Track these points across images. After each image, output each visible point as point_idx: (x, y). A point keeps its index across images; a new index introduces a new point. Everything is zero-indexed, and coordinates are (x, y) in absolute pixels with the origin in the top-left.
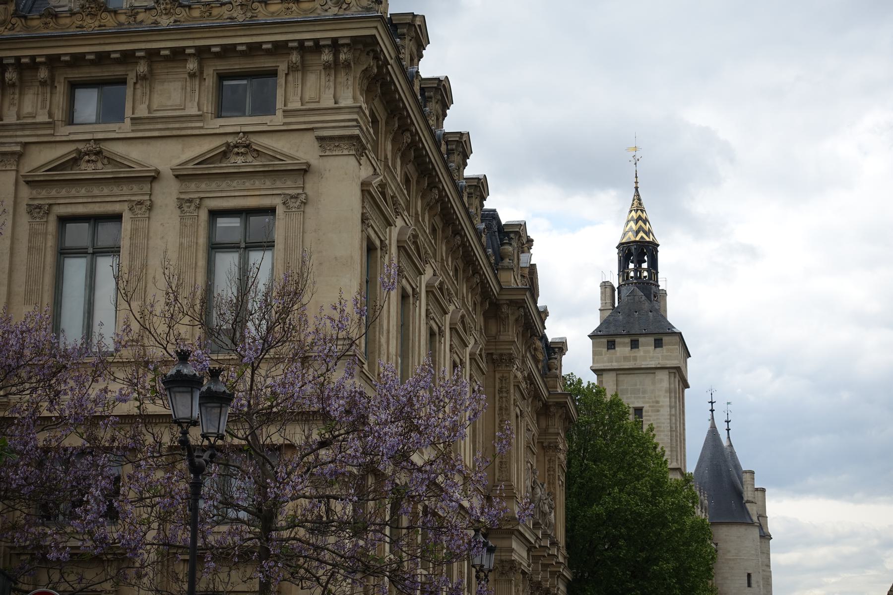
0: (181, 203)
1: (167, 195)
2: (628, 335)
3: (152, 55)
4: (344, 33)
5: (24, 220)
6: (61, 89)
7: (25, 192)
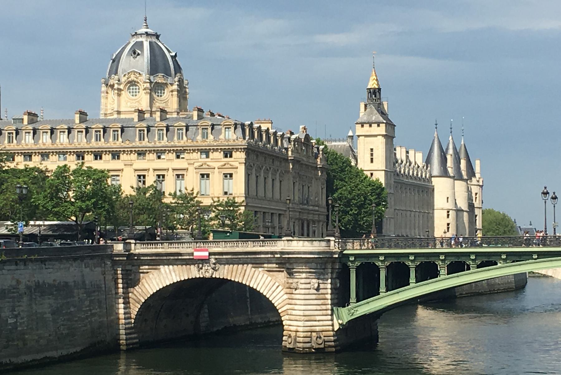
0: (219, 172)
1: (216, 170)
2: (368, 123)
3: (213, 149)
4: (242, 147)
5: (195, 174)
6: (199, 153)
7: (195, 170)
